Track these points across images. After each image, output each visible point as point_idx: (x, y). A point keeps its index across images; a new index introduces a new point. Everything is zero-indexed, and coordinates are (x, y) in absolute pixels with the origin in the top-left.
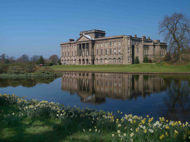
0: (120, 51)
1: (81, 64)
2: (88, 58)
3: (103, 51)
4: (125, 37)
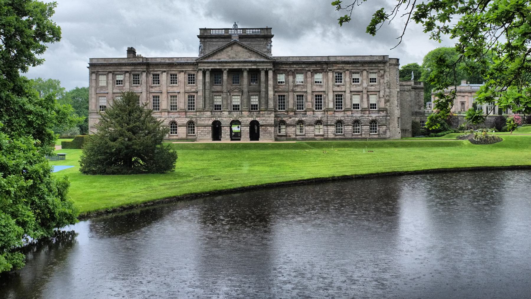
0: (373, 99)
1: (226, 139)
2: (257, 119)
3: (309, 98)
4: (391, 62)
